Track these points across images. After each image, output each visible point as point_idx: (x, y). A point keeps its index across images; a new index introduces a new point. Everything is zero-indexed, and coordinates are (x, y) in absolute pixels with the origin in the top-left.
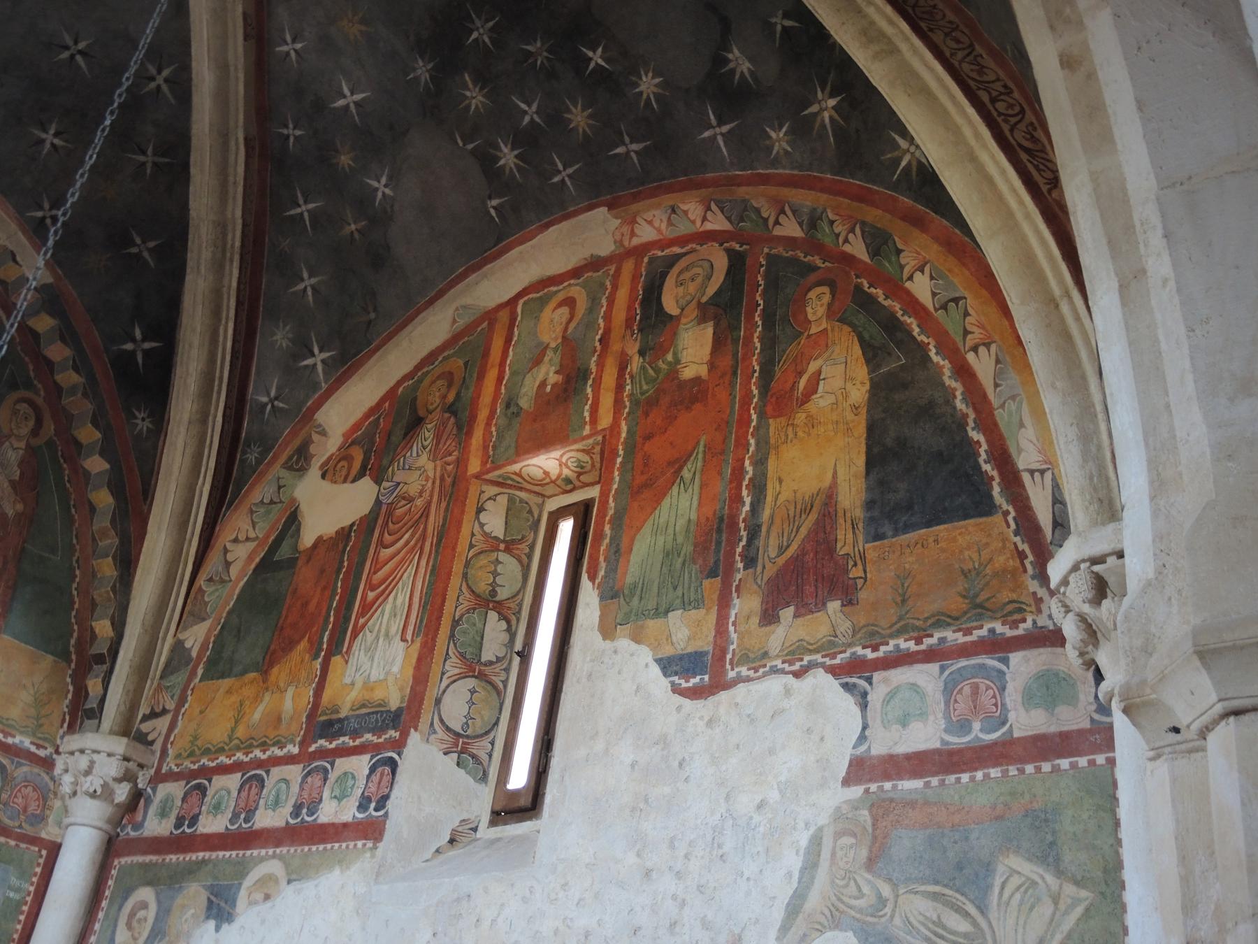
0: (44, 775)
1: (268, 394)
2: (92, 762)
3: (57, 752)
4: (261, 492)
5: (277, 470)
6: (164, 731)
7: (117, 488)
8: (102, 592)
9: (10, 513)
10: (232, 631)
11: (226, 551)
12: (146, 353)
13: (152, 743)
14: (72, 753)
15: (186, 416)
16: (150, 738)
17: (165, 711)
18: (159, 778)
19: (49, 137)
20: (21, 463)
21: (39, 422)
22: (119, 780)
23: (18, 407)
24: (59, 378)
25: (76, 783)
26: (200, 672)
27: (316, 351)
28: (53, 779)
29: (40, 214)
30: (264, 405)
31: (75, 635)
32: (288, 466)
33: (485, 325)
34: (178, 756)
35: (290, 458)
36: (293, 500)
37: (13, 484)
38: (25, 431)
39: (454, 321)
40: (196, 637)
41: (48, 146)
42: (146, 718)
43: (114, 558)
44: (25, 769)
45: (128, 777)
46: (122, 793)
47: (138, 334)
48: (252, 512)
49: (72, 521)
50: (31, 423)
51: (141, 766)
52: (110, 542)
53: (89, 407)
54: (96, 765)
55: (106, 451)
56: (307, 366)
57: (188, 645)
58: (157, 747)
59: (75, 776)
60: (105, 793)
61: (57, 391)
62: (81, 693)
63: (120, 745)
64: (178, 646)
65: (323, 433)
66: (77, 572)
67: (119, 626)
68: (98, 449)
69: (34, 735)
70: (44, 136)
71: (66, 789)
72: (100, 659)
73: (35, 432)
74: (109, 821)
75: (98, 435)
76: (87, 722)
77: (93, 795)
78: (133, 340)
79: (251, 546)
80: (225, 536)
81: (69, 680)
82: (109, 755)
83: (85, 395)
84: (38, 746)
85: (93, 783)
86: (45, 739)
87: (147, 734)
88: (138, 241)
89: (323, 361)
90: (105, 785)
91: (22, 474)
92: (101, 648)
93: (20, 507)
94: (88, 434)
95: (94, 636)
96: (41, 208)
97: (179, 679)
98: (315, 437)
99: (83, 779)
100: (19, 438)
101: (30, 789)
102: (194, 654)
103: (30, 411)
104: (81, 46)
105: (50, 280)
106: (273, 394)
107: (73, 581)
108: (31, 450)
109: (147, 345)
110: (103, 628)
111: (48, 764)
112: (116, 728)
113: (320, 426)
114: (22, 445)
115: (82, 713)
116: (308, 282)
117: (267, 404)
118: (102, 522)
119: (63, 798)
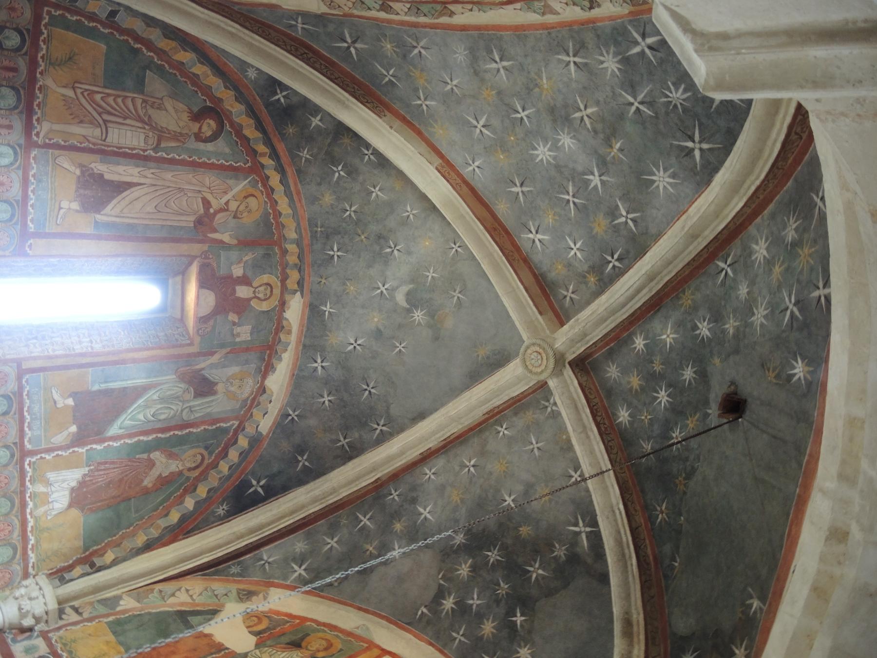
0: (19, 578)
1: (269, 558)
2: (37, 598)
3: (34, 577)
4: (218, 587)
5: (233, 588)
6: (70, 621)
7: (183, 519)
8: (128, 545)
9: (145, 483)
10: (139, 620)
11: (179, 590)
12: (256, 491)
13: (61, 618)
14: (37, 584)
15: (236, 529)
16: (64, 616)
17: (80, 614)
18: (44, 635)
19: (326, 399)
20: (171, 473)
22: (34, 617)
24: (222, 462)
25: (22, 596)
26: (111, 619)
27: (303, 567)
28: (20, 582)
29: (291, 412)
30: (262, 559)
32: (239, 592)
33: (366, 645)
34: (61, 638)
35: (244, 590)
36: (223, 606)
39: (358, 628)
40: (128, 604)
41: (322, 400)
42: (73, 607)
43: (148, 540)
44: (18, 568)
45: (38, 620)
46: (28, 622)
47: (262, 483)
48: (206, 589)
50: (194, 465)
51: (47, 622)
52: (154, 533)
53: (215, 484)
54: (36, 601)
55: (197, 503)
56: (293, 568)
57: (122, 602)
58: (61, 623)
59: (26, 594)
60: (23, 615)
61: (214, 465)
62: (70, 568)
63: (53, 605)
64: (118, 598)
65: (265, 598)
67: (115, 563)
68: (198, 499)
69: (38, 561)
70: (326, 396)
71: (17, 594)
72: (93, 565)
73: (190, 469)
74: (10, 624)
76: (57, 580)
77: (20, 609)
78: (258, 482)
79: (189, 600)
80: (187, 583)
81: (74, 558)
82: (45, 604)
83: (220, 479)
84: (33, 567)
85: (27, 605)
86: (38, 567)
87: (65, 613)
88: (305, 457)
89: (300, 574)
90: (28, 612)
92: (98, 562)
93: (150, 485)
94: (202, 491)
95: (102, 555)
96: (294, 412)
97: (102, 610)
98: (261, 596)
99: (26, 598)
100: (183, 465)
101: (9, 576)
102: (119, 609)
103: (199, 461)
104: (373, 391)
105: (264, 433)
106: (270, 560)
108: (180, 473)
109: (260, 490)
110: (109, 556)
111: (26, 575)
112: (60, 598)
113: (267, 594)
114: (181, 468)
115: (60, 575)
116: (333, 543)
117: (263, 560)
118: (163, 523)
119: (11, 593)
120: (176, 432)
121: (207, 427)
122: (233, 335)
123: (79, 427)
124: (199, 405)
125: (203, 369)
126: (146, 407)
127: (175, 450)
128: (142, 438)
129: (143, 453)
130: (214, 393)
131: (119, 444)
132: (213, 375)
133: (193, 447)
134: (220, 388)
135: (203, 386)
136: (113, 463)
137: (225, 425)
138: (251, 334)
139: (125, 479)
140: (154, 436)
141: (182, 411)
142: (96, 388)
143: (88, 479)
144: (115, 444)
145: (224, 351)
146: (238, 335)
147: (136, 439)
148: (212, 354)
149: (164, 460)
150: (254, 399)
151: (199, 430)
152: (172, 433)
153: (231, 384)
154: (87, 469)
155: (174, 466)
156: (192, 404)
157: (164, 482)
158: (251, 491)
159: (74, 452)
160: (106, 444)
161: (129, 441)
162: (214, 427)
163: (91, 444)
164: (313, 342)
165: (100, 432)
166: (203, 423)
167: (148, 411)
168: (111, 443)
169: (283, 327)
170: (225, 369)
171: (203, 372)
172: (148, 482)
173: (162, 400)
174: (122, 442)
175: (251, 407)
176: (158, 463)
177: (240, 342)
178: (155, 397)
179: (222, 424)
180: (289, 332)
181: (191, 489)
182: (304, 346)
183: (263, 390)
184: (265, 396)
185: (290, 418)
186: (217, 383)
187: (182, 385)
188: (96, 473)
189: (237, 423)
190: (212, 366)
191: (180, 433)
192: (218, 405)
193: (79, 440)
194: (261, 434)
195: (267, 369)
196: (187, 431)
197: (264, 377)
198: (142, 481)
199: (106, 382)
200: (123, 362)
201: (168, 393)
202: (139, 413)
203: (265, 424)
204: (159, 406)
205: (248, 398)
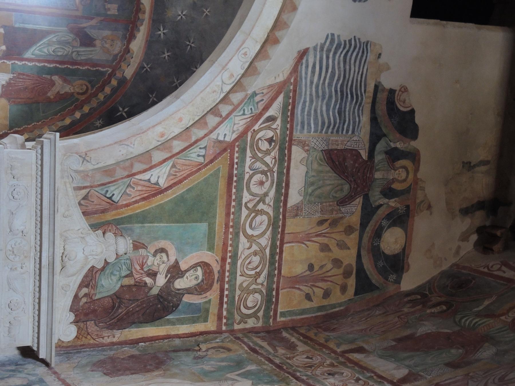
7: (73, 124)
12: (122, 114)
19: (166, 54)
21: (82, 94)
23: (84, 86)
24: (100, 94)
29: (146, 66)
31: (19, 129)
37: (58, 92)
38: (77, 90)
41: (164, 56)
47: (126, 110)
49: (56, 115)
50: (81, 91)
53: (95, 105)
61: (95, 95)
66: (40, 123)
70: (166, 53)
73: (78, 93)
75: (87, 111)
78: (123, 109)
81: (4, 132)
83: (98, 103)
88: (154, 95)
91: (63, 94)
93: (52, 97)
94: (86, 109)
96: (147, 65)
100: (74, 89)
104: (193, 45)
107: (37, 122)
108: (72, 94)
114: (72, 91)
120: (69, 66)
121: (89, 68)
122: (105, 9)
123: (7, 48)
124: (84, 51)
125: (85, 28)
126: (49, 44)
127: (69, 78)
128: (46, 64)
129: (47, 74)
130: (94, 46)
131: (31, 64)
132: (93, 33)
133: (80, 79)
134: (98, 43)
135: (87, 41)
136: (27, 76)
137: (102, 70)
138: (118, 10)
139: (36, 88)
140: (54, 65)
141: (72, 52)
142: (17, 25)
143: (12, 82)
144: (29, 64)
145: (100, 18)
146: (109, 9)
147: (43, 64)
148: (92, 19)
149: (61, 83)
150: (122, 56)
151: (84, 68)
152: (66, 66)
153: (106, 42)
154: (12, 75)
155: (68, 89)
156: (78, 49)
157: (62, 98)
158: (118, 114)
159: (4, 62)
160: (24, 62)
161: (37, 64)
162: (95, 69)
163: (14, 60)
164: (158, 18)
165: (20, 54)
166: (86, 64)
167: (50, 48)
168: (27, 63)
169: (141, 9)
170: (101, 31)
171: (85, 30)
172: (51, 94)
173: (59, 42)
174: (34, 63)
175: (120, 61)
176: (57, 84)
177: (111, 15)
178: (54, 40)
179: (100, 69)
180: (144, 13)
181: (80, 107)
182: (153, 21)
183: (127, 50)
184: (129, 54)
185: (145, 69)
186: (95, 40)
187: (72, 35)
188: (18, 80)
189: (110, 70)
190: (92, 27)
191: (71, 67)
192: (96, 54)
193: (8, 55)
194: (125, 78)
195: (132, 37)
196: (76, 67)
197: (129, 42)
198: (47, 93)
199: (23, 23)
200: (34, 13)
201: (63, 39)
202: (44, 47)
203: (129, 72)
204: (57, 46)
205: (118, 54)
